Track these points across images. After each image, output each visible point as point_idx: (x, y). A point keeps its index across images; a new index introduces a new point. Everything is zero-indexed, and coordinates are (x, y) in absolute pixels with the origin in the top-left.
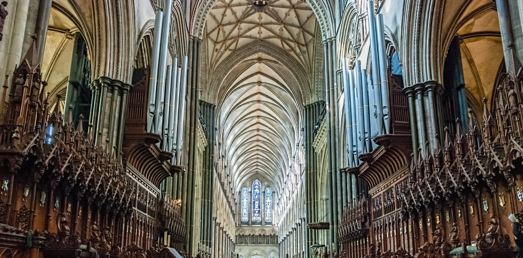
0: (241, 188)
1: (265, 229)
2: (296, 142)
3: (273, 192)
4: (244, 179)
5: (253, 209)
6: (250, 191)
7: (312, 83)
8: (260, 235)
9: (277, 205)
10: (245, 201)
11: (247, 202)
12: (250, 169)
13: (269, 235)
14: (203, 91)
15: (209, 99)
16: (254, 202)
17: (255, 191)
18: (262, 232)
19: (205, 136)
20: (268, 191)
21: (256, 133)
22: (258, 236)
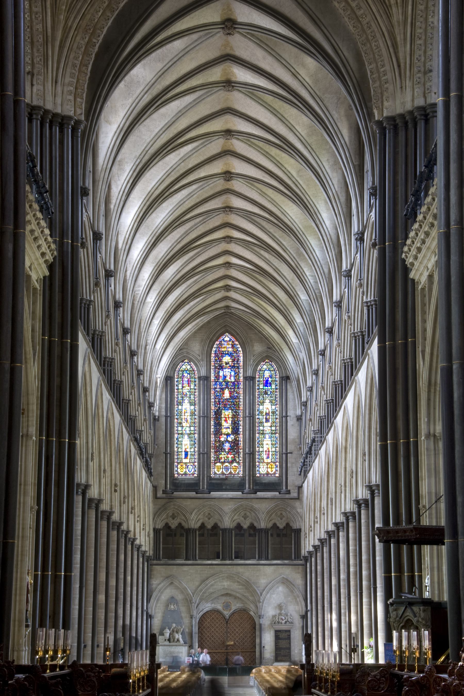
0: (173, 365)
1: (257, 505)
2: (355, 228)
3: (282, 378)
4: (182, 334)
5: (213, 438)
6: (203, 373)
7: (405, 39)
8: (239, 527)
9: (297, 424)
10: (186, 407)
11: (193, 414)
12: (203, 300)
13: (270, 525)
14: (35, 71)
15: (59, 101)
16: (218, 414)
18: (245, 517)
19: (47, 231)
20: (267, 374)
21: (220, 184)
22: (230, 530)
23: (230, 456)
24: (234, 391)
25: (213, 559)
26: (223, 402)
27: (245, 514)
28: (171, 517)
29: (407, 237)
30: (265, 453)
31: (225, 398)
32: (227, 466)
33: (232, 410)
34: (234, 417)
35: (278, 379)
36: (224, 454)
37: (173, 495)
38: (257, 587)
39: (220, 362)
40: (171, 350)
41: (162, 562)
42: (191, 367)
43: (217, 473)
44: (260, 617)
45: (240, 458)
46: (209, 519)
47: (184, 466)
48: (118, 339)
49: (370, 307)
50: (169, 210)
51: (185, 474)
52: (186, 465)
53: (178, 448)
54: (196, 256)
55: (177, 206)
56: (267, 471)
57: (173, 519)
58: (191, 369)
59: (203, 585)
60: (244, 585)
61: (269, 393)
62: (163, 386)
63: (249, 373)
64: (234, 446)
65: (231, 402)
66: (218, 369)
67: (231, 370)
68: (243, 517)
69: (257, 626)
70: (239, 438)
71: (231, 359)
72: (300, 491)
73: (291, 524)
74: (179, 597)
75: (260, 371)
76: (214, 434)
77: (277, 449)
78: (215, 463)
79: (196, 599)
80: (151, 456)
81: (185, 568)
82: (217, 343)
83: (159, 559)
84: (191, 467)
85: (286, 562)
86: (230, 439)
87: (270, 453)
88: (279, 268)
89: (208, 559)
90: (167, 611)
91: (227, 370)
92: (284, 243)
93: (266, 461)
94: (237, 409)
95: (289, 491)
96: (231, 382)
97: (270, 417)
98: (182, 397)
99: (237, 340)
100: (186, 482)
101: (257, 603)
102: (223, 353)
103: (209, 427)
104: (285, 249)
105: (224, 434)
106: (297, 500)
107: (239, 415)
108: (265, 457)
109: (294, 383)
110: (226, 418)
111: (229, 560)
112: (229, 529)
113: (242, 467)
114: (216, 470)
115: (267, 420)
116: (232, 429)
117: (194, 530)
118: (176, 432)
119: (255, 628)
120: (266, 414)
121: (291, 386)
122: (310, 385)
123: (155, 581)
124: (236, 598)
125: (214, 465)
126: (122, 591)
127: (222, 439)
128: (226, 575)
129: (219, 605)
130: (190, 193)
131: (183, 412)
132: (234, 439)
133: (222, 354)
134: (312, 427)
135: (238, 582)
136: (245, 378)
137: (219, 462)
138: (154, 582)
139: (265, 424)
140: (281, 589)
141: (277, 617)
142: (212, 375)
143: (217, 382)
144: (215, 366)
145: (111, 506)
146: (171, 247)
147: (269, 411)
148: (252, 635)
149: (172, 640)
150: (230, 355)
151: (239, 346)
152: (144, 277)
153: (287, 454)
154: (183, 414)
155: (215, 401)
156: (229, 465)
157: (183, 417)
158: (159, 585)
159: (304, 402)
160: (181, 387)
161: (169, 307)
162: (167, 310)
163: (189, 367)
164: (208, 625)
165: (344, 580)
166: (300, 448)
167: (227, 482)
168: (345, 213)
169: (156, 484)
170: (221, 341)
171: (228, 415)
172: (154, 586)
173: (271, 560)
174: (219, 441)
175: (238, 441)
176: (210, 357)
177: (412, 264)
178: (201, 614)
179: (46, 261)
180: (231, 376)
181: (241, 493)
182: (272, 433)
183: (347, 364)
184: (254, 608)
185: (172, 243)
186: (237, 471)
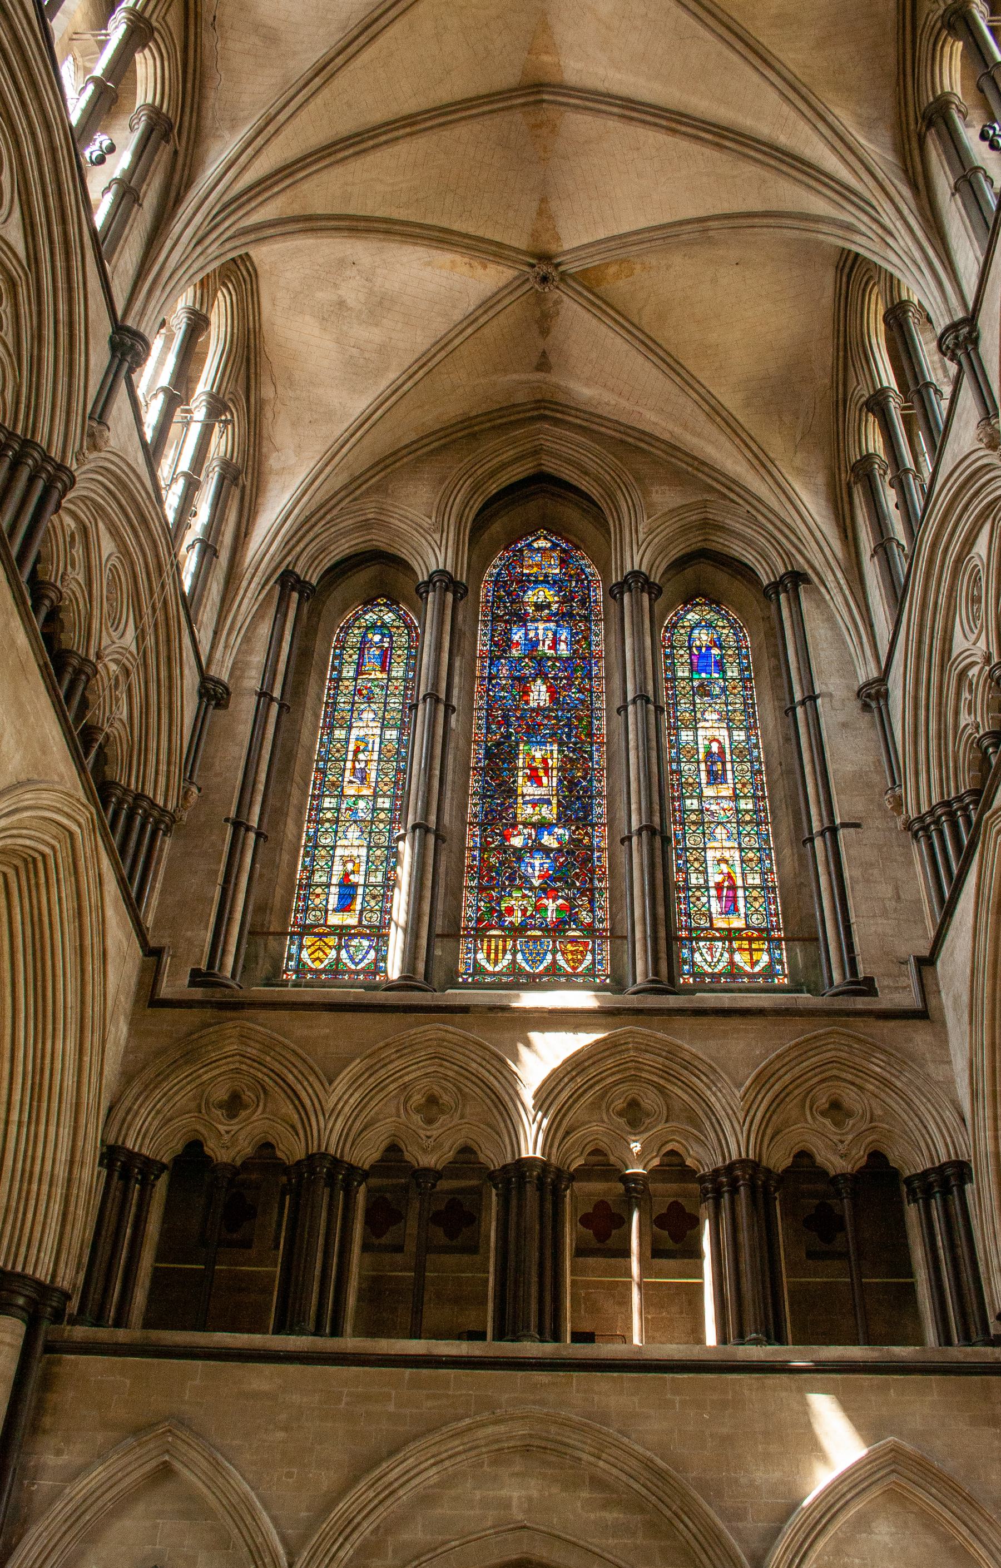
9: (864, 721)
13: (779, 1160)
28: (220, 1106)
30: (713, 892)
31: (533, 704)
33: (561, 744)
36: (524, 896)
38: (735, 1516)
39: (512, 602)
43: (490, 968)
45: (599, 913)
46: (430, 1121)
53: (313, 872)
56: (732, 963)
58: (396, 624)
59: (362, 1492)
60: (636, 1504)
64: (568, 866)
65: (556, 718)
66: (506, 622)
70: (591, 837)
72: (928, 981)
76: (480, 824)
77: (769, 877)
86: (548, 840)
87: (740, 893)
91: (541, 626)
95: (869, 981)
96: (558, 659)
97: (729, 766)
106: (919, 1023)
107: (591, 758)
108: (715, 906)
110: (535, 770)
115: (715, 778)
116: (559, 804)
120: (709, 754)
123: (59, 1453)
131: (352, 747)
132: (572, 840)
135: (597, 1483)
139: (708, 792)
143: (499, 658)
147: (721, 748)
150: (556, 584)
153: (833, 830)
154: (350, 756)
155: (488, 715)
158: (75, 1474)
160: (351, 674)
166: (899, 803)
170: (521, 551)
171: (544, 760)
172: (45, 1484)
174: (503, 849)
180: (555, 642)
186: (587, 963)
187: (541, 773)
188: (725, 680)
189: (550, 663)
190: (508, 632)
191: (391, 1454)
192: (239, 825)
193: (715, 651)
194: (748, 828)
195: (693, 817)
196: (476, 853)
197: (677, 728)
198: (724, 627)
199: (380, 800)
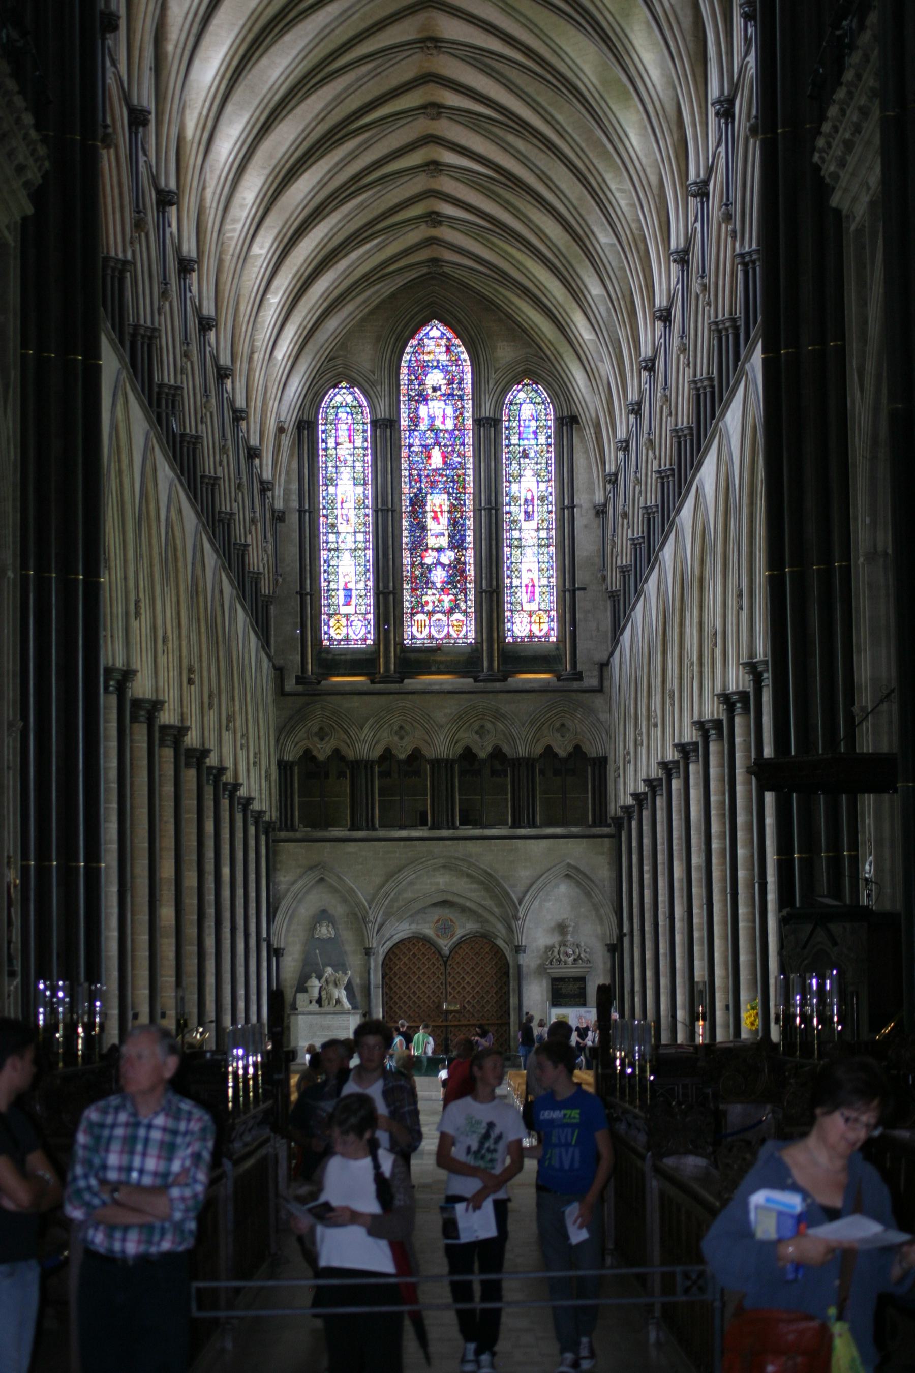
2: (714, 91)
4: (332, 324)
6: (383, 412)
8: (468, 754)
9: (596, 523)
11: (360, 505)
13: (539, 750)
16: (418, 503)
17: (423, 411)
19: (28, 119)
20: (527, 411)
23: (446, 599)
24: (453, 451)
25: (413, 826)
26: (427, 476)
27: (482, 727)
28: (316, 734)
29: (822, 118)
30: (524, 589)
31: (434, 467)
32: (439, 620)
33: (449, 494)
34: (453, 509)
35: (550, 423)
36: (434, 594)
37: (319, 687)
39: (419, 385)
40: (309, 360)
41: (298, 835)
42: (355, 398)
43: (418, 635)
44: (518, 949)
45: (469, 603)
46: (402, 738)
47: (343, 621)
48: (188, 344)
49: (751, 266)
50: (299, 48)
51: (347, 639)
52: (347, 620)
53: (329, 582)
54: (362, 149)
55: (317, 40)
56: (531, 631)
57: (322, 739)
58: (355, 403)
59: (390, 884)
61: (532, 455)
62: (293, 444)
63: (487, 411)
66: (417, 401)
67: (446, 404)
68: (477, 733)
69: (511, 971)
71: (445, 378)
72: (605, 674)
73: (585, 749)
74: (339, 910)
75: (511, 404)
76: (410, 549)
77: (551, 580)
78: (413, 615)
79: (376, 915)
80: (268, 601)
81: (351, 847)
82: (414, 342)
83: (293, 829)
84: (360, 624)
85: (575, 830)
87: (537, 590)
88: (549, 173)
89: (402, 827)
90: (311, 940)
92: (559, 117)
93: (527, 607)
94: (460, 493)
95: (581, 673)
96: (446, 431)
97: (536, 507)
98: (337, 467)
99: (458, 336)
100: (349, 657)
101: (511, 919)
102: (428, 366)
103: (397, 532)
104: (561, 130)
105: (432, 549)
106: (599, 694)
107: (465, 505)
108: (523, 596)
109: (589, 432)
110: (435, 512)
111: (449, 829)
112: (447, 760)
113: (473, 622)
114: (414, 629)
115: (528, 516)
116: (449, 536)
117: (368, 765)
118: (323, 545)
119: (507, 974)
120: (526, 500)
121: (582, 439)
122: (624, 436)
123: (285, 876)
124: (464, 909)
125: (411, 619)
126: (212, 897)
127: (428, 561)
128: (442, 861)
129: (427, 925)
130: (345, 11)
131: (339, 501)
132: (456, 559)
133: (423, 367)
134: (630, 531)
135: (469, 876)
136: (478, 422)
137: (423, 613)
138: (283, 879)
139: (525, 525)
140: (564, 889)
141: (556, 950)
142: (404, 415)
143: (414, 430)
144: (409, 395)
145: (182, 714)
146: (303, 131)
147: (533, 496)
148: (501, 988)
149: (325, 1002)
151: (462, 349)
152: (244, 199)
154: (339, 505)
155: (410, 475)
156: (445, 619)
157: (339, 512)
158: (293, 883)
159: (610, 475)
160: (333, 445)
161: (302, 265)
162: (298, 271)
163: (349, 399)
164: (405, 969)
165: (699, 868)
166: (604, 578)
167: (439, 657)
168: (692, 53)
169: (280, 662)
170: (422, 339)
171: (441, 506)
172: (282, 887)
173: (540, 827)
174: (422, 565)
175: (465, 563)
176: (398, 374)
177: (836, 177)
178: (389, 944)
179: (26, 184)
181: (471, 680)
182: (540, 546)
183: (702, 391)
184: (503, 931)
185: (307, 121)
186: (464, 632)
187: (439, 514)
188: (537, 445)
189: (442, 435)
190: (417, 409)
191: (399, 871)
192: (302, 595)
193: (533, 424)
194: (543, 549)
195: (516, 543)
196: (409, 568)
197: (510, 482)
198: (539, 404)
199: (358, 535)
